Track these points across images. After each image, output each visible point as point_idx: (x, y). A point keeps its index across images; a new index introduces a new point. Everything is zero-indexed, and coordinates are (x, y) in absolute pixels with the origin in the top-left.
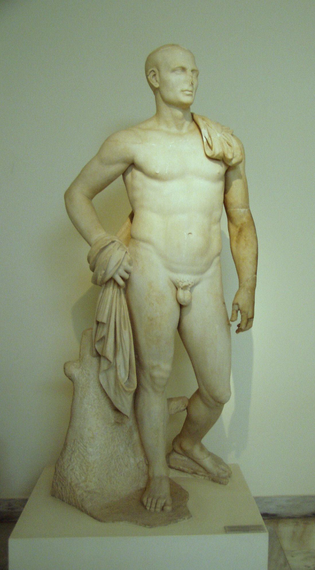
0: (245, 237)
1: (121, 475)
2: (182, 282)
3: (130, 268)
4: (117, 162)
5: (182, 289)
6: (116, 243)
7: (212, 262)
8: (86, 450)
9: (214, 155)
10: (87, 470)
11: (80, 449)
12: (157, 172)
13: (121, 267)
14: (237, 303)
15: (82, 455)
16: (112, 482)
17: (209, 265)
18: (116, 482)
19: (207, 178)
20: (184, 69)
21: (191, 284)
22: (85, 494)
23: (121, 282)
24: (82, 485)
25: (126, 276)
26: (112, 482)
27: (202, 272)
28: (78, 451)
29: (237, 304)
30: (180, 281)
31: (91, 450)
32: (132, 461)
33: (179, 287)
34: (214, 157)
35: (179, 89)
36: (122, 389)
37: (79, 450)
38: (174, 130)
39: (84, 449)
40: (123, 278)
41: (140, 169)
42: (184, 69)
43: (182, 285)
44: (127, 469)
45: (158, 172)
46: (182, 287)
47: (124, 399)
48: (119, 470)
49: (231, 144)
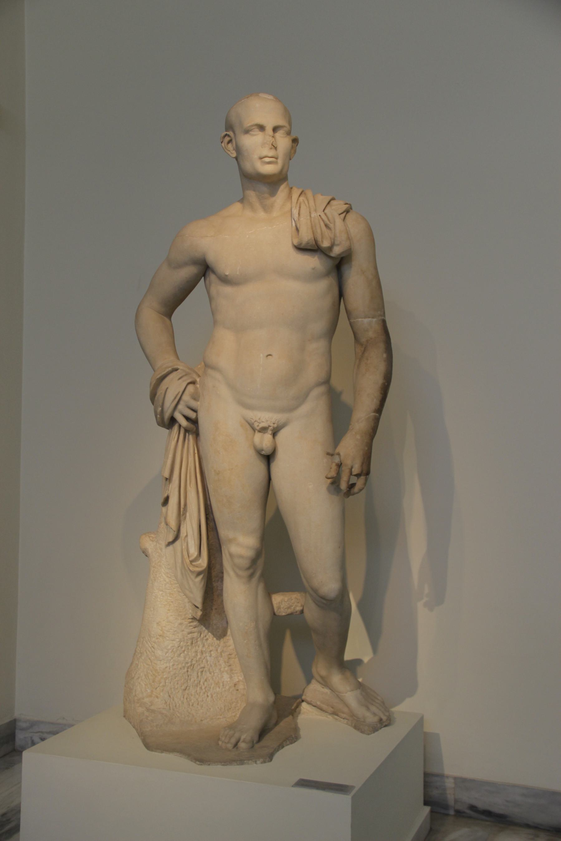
0: (367, 359)
1: (208, 696)
2: (258, 422)
3: (193, 404)
4: (185, 264)
5: (259, 431)
6: (179, 371)
7: (307, 395)
8: (154, 652)
9: (301, 244)
10: (154, 681)
11: (147, 651)
12: (226, 274)
13: (182, 402)
14: (338, 452)
15: (150, 659)
16: (191, 704)
17: (301, 399)
18: (198, 704)
19: (296, 277)
20: (262, 128)
21: (272, 425)
22: (146, 713)
23: (184, 423)
24: (146, 700)
25: (192, 415)
26: (191, 704)
27: (291, 409)
28: (145, 653)
29: (339, 454)
30: (256, 421)
31: (159, 653)
32: (226, 677)
33: (256, 429)
34: (302, 246)
35: (256, 157)
36: (187, 568)
37: (146, 653)
38: (262, 214)
39: (152, 651)
40: (187, 418)
41: (214, 272)
42: (262, 128)
43: (258, 426)
44: (218, 689)
45: (227, 274)
46: (258, 428)
47: (191, 582)
48: (203, 687)
49: (331, 226)
